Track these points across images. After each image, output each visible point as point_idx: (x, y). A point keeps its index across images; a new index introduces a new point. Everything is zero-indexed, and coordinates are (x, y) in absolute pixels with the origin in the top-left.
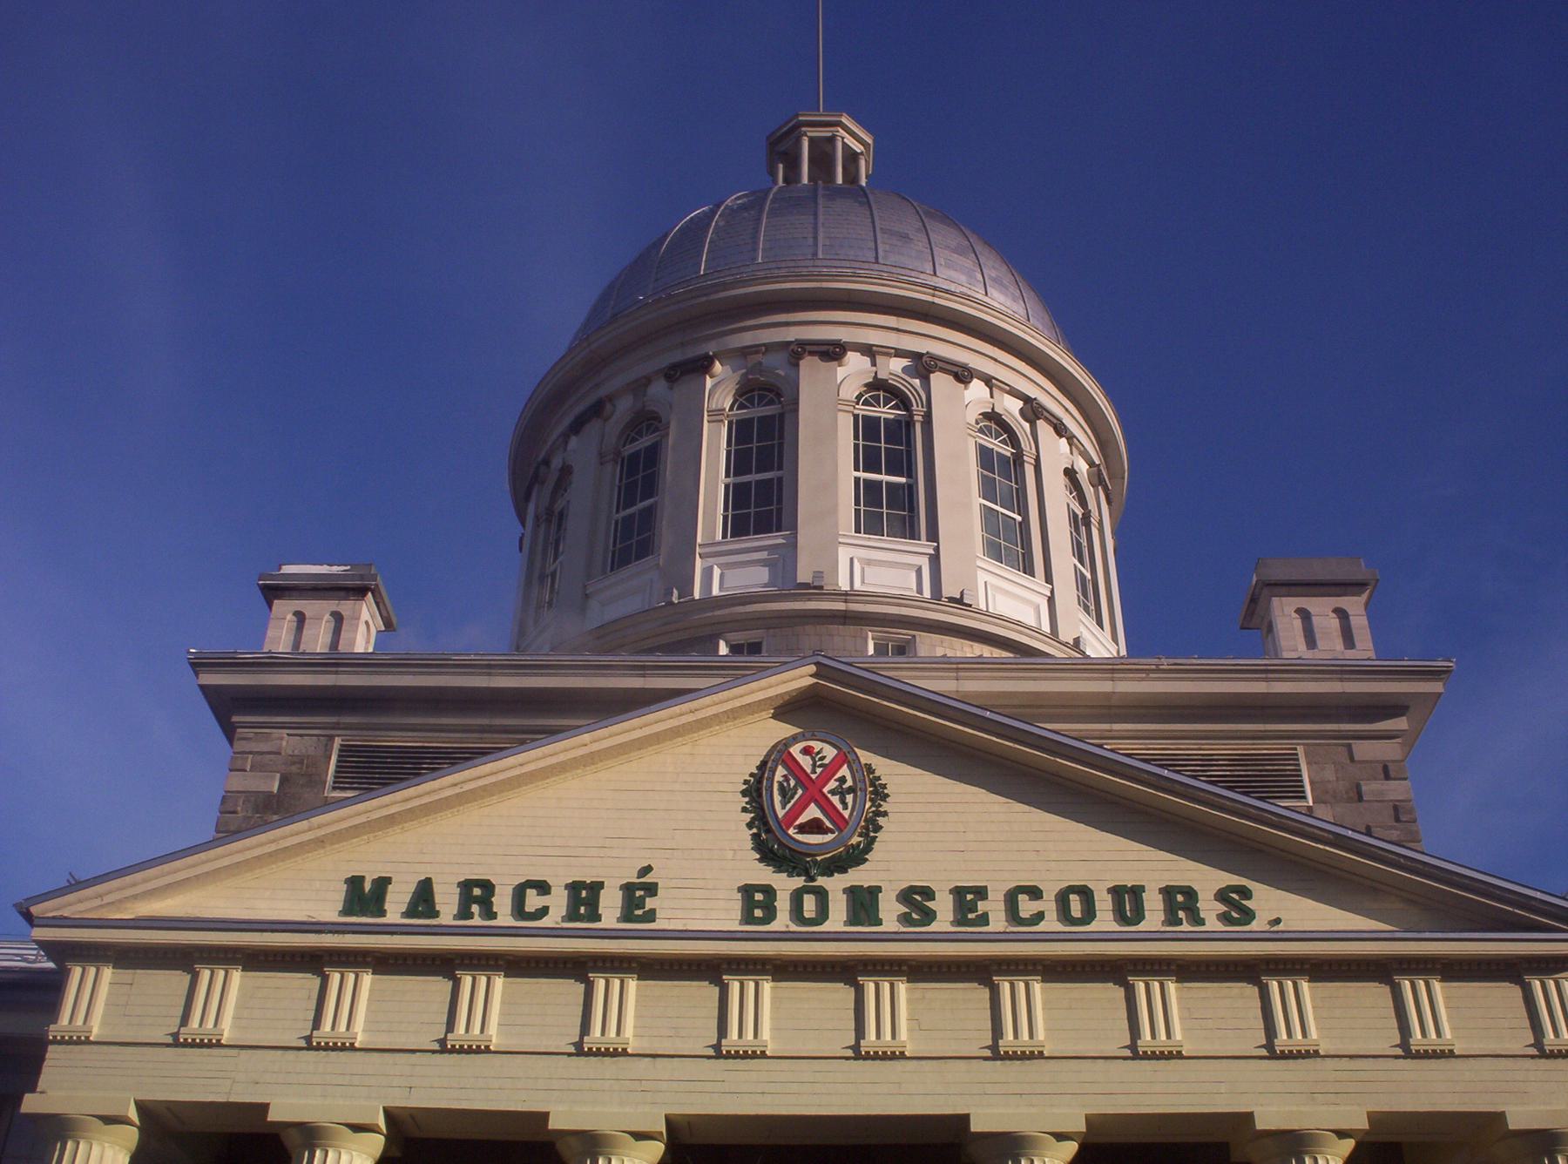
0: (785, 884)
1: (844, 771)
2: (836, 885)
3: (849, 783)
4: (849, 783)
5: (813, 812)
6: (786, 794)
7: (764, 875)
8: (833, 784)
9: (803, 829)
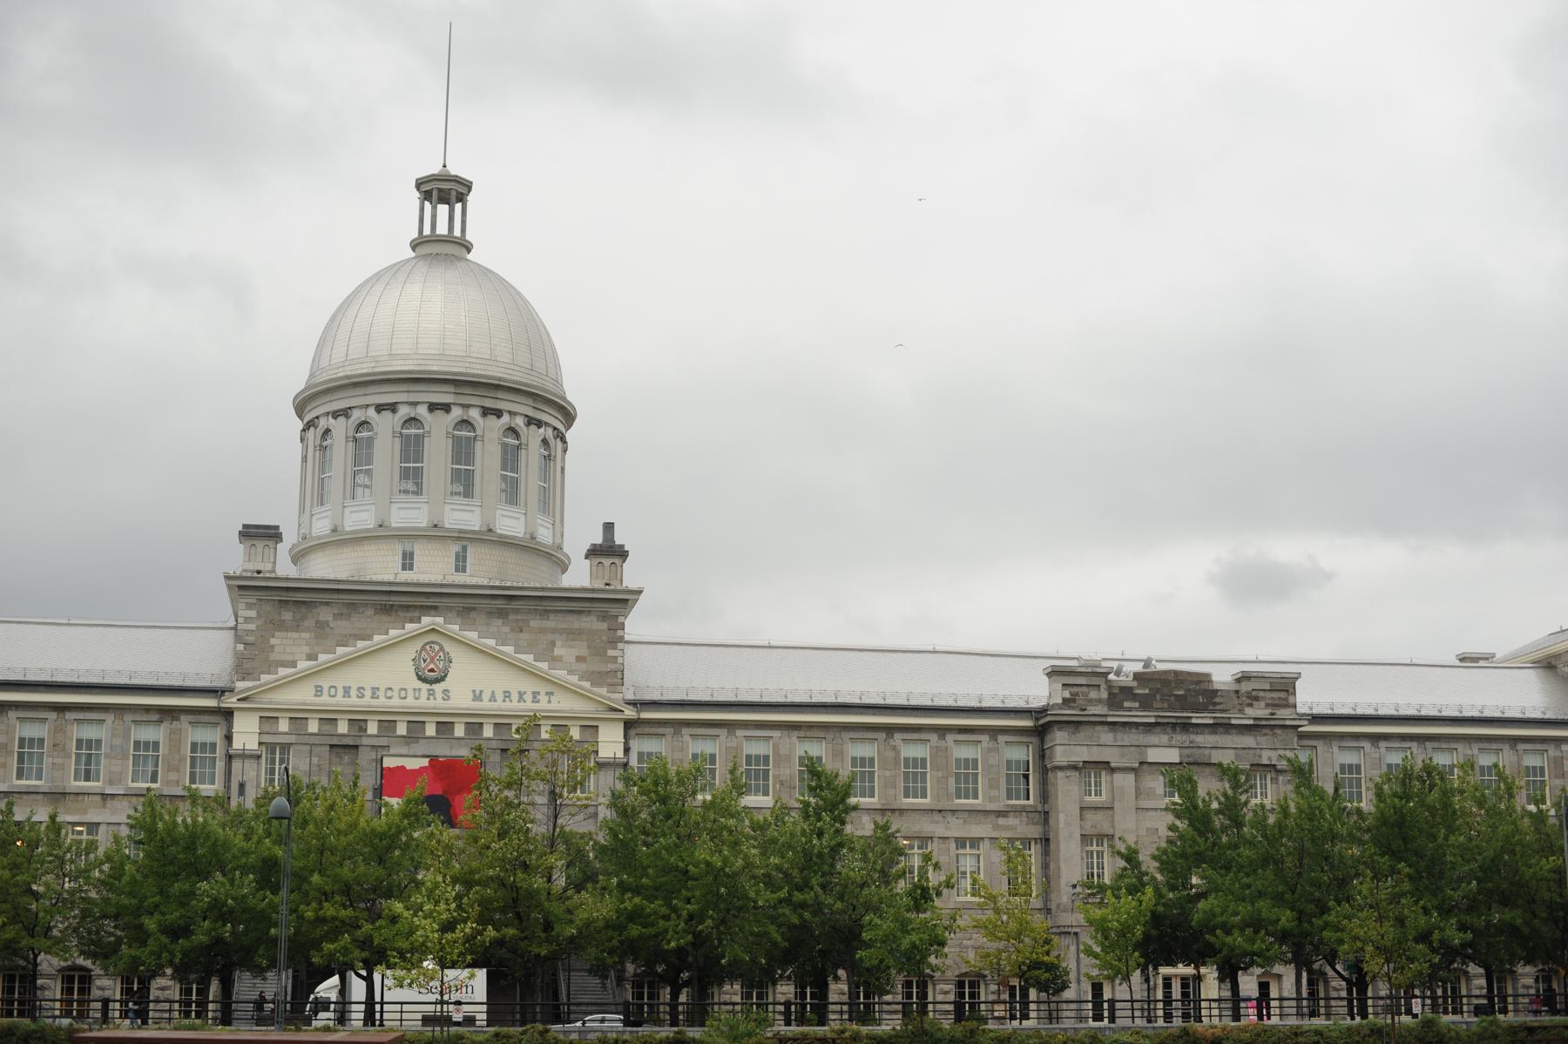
0: (425, 687)
1: (441, 654)
2: (438, 688)
3: (442, 658)
4: (442, 658)
5: (432, 666)
6: (425, 661)
7: (420, 684)
8: (438, 658)
9: (429, 671)
